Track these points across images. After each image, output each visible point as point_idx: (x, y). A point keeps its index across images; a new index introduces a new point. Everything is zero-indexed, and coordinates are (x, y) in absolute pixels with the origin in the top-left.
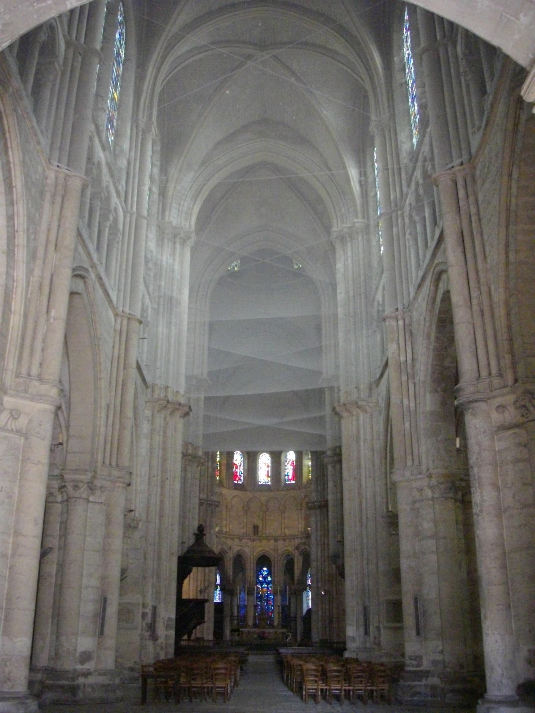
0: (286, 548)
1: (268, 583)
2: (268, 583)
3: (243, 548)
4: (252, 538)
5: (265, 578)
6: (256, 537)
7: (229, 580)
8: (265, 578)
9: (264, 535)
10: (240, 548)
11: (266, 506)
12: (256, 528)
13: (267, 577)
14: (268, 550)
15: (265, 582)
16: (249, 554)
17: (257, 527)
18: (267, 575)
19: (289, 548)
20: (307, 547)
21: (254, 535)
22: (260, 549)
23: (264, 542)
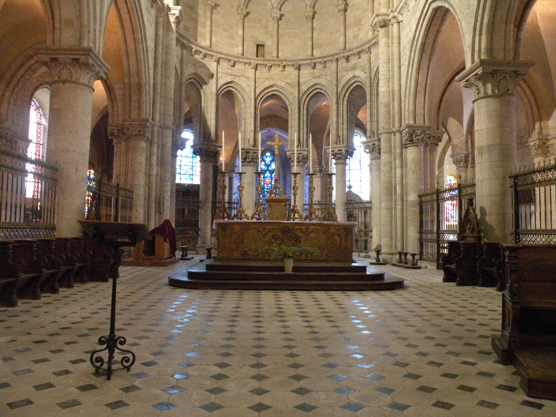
0: (316, 81)
1: (272, 172)
2: (272, 172)
3: (236, 80)
4: (252, 61)
5: (268, 166)
6: (260, 61)
7: (210, 135)
8: (268, 166)
9: (275, 58)
10: (229, 79)
11: (280, 10)
12: (260, 47)
13: (270, 165)
14: (283, 84)
15: (268, 170)
16: (247, 90)
17: (263, 46)
18: (271, 161)
19: (322, 81)
20: (358, 73)
21: (257, 56)
22: (267, 84)
23: (276, 71)
